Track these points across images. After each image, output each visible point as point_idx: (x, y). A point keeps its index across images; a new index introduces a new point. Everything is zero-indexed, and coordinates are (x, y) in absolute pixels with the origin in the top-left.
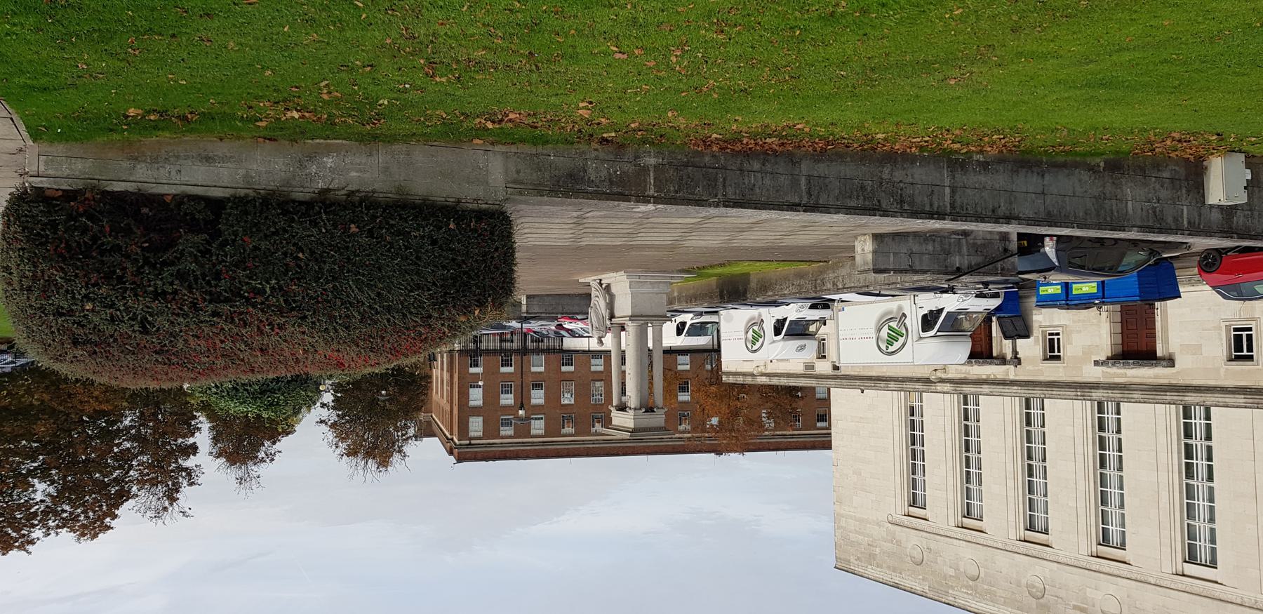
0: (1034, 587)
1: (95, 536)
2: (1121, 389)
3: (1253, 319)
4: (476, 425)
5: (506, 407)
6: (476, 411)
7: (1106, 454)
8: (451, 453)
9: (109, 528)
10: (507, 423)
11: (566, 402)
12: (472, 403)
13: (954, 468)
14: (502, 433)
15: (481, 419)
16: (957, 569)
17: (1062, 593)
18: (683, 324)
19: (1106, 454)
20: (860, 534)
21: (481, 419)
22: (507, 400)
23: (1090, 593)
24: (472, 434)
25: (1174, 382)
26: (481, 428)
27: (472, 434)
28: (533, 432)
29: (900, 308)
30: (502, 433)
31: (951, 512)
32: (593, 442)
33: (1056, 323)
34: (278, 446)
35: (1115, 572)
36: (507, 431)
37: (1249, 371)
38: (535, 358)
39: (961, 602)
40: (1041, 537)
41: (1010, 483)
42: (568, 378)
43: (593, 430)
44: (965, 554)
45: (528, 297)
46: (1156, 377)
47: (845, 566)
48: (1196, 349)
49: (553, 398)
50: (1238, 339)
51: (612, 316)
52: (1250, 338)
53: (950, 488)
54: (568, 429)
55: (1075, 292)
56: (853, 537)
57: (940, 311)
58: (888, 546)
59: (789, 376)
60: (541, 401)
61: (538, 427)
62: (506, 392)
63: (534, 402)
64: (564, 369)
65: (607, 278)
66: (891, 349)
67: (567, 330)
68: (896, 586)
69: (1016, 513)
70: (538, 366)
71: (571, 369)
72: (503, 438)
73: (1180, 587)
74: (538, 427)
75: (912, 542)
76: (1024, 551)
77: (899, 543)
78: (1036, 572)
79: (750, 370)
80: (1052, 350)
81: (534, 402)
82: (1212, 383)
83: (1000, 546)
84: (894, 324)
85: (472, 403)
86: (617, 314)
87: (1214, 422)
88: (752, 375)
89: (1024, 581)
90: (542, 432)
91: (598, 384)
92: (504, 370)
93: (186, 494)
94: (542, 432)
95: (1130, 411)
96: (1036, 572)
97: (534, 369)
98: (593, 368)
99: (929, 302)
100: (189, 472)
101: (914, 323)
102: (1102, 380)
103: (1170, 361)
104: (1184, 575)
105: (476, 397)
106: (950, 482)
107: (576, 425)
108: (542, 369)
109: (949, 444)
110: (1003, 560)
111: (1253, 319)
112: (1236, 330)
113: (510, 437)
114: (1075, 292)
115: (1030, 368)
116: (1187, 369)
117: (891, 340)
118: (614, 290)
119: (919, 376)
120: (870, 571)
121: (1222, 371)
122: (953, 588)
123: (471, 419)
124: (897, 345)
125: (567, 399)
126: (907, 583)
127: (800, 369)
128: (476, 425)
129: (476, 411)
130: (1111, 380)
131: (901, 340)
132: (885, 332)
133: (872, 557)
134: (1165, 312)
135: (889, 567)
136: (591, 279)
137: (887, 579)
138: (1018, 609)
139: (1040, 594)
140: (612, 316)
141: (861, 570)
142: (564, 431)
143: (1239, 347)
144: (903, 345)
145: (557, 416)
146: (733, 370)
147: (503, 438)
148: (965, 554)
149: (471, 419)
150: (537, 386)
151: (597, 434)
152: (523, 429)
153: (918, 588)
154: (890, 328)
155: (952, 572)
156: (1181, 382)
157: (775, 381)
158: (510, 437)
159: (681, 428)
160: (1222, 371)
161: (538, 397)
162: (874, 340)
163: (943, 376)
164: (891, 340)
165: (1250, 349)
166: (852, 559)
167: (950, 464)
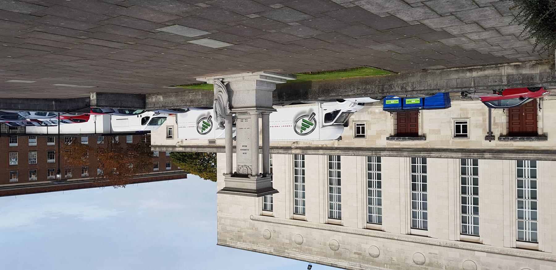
0: (333, 245)
2: (397, 151)
3: (467, 118)
7: (374, 180)
11: (13, 164)
13: (290, 191)
16: (290, 240)
17: (349, 247)
18: (148, 118)
19: (374, 180)
20: (233, 226)
23: (363, 246)
25: (425, 147)
29: (209, 113)
31: (288, 212)
32: (30, 185)
33: (362, 119)
35: (377, 235)
37: (464, 142)
39: (292, 256)
40: (378, 226)
41: (321, 196)
42: (14, 150)
43: (30, 179)
44: (296, 232)
45: (98, 94)
47: (223, 243)
48: (438, 132)
50: (458, 128)
51: (231, 107)
52: (363, 128)
53: (287, 201)
55: (407, 103)
56: (228, 228)
57: (337, 112)
58: (250, 231)
59: (198, 147)
64: (11, 145)
65: (229, 78)
66: (304, 132)
68: (255, 251)
69: (324, 210)
71: (16, 144)
73: (410, 240)
75: (264, 228)
76: (329, 228)
77: (257, 229)
78: (335, 238)
79: (174, 145)
80: (358, 132)
83: (315, 227)
84: (306, 119)
86: (234, 104)
87: (342, 162)
88: (175, 147)
89: (328, 243)
91: (33, 153)
95: (385, 161)
96: (335, 238)
98: (30, 144)
99: (331, 107)
101: (320, 117)
102: (387, 147)
103: (424, 137)
104: (411, 234)
106: (287, 197)
107: (19, 177)
109: (287, 179)
110: (316, 234)
111: (467, 118)
112: (457, 123)
114: (407, 103)
115: (347, 141)
117: (304, 127)
118: (233, 87)
119: (282, 146)
120: (239, 244)
121: (451, 142)
122: (287, 249)
124: (308, 130)
126: (262, 248)
127: (206, 143)
130: (392, 147)
131: (311, 127)
132: (300, 123)
133: (239, 238)
134: (422, 114)
135: (250, 242)
136: (210, 80)
137: (249, 247)
138: (324, 256)
139: (336, 248)
140: (231, 107)
141: (233, 245)
142: (11, 180)
144: (313, 130)
146: (160, 144)
148: (296, 232)
151: (32, 181)
153: (268, 251)
154: (304, 121)
155: (287, 241)
156: (429, 147)
157: (188, 150)
159: (83, 175)
160: (451, 142)
162: (293, 127)
163: (298, 146)
164: (304, 127)
165: (363, 132)
166: (228, 239)
167: (287, 188)
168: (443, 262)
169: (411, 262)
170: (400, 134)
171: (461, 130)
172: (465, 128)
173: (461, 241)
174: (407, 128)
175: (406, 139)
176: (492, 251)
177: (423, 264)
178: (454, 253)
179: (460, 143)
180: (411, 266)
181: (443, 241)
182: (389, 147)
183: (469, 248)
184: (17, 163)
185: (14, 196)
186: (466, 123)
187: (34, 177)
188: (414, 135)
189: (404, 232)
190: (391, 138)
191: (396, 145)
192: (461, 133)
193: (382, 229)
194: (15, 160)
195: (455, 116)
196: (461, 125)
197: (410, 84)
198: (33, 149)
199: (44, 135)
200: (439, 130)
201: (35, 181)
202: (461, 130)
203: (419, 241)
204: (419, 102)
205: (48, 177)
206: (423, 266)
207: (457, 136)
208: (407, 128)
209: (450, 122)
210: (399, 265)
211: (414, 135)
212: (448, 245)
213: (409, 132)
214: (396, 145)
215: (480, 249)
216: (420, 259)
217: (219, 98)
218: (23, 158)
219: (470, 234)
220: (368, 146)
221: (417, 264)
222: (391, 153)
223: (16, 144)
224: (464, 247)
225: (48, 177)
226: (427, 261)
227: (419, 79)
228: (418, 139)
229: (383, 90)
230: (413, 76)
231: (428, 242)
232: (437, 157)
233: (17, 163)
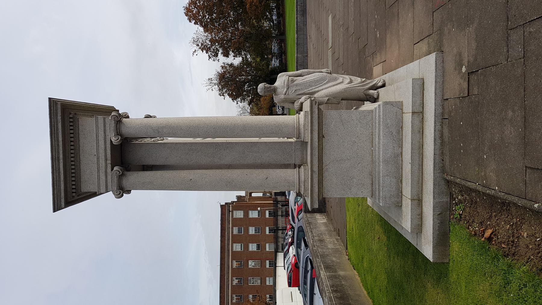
1: (187, 15)
4: (239, 214)
5: (248, 230)
6: (246, 214)
8: (226, 203)
9: (190, 21)
10: (240, 231)
11: (250, 263)
12: (250, 212)
14: (235, 228)
15: (242, 217)
21: (242, 217)
22: (252, 231)
24: (235, 212)
26: (237, 217)
27: (235, 212)
28: (235, 245)
30: (235, 228)
34: (227, 97)
36: (236, 231)
38: (273, 246)
42: (263, 264)
43: (234, 278)
49: (252, 256)
54: (235, 264)
60: (250, 249)
61: (237, 247)
62: (256, 230)
63: (250, 245)
64: (268, 262)
67: (288, 250)
70: (269, 248)
71: (268, 266)
72: (232, 228)
74: (237, 247)
81: (250, 245)
85: (250, 212)
90: (234, 250)
91: (259, 281)
92: (267, 229)
93: (204, 55)
94: (234, 250)
97: (267, 245)
98: (267, 279)
100: (216, 55)
105: (253, 214)
107: (237, 268)
108: (267, 249)
113: (232, 232)
123: (242, 212)
125: (251, 264)
128: (239, 214)
129: (246, 214)
145: (243, 257)
147: (232, 228)
149: (242, 212)
150: (258, 247)
151: (232, 280)
152: (236, 239)
158: (232, 232)
161: (253, 247)
184: (250, 267)
185: (219, 264)
187: (236, 282)
194: (253, 265)
198: (263, 281)
199: (276, 264)
201: (232, 283)
205: (234, 296)
217: (336, 79)
218: (255, 273)
223: (268, 266)
225: (234, 296)
233: (250, 267)
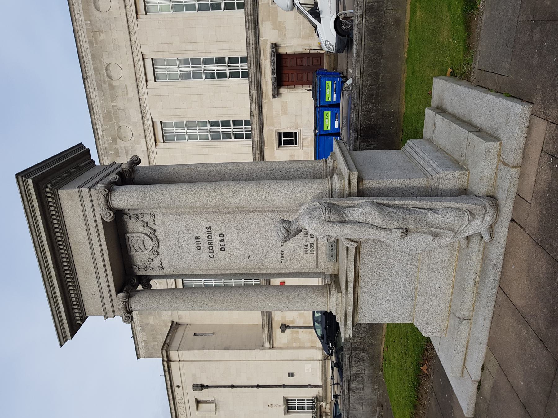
2: (256, 58)
25: (264, 96)
35: (128, 8)
37: (273, 143)
46: (266, 83)
48: (284, 112)
50: (289, 135)
55: (325, 113)
73: (136, 59)
82: (265, 121)
102: (261, 39)
103: (276, 94)
112: (296, 133)
114: (325, 113)
116: (272, 106)
121: (272, 128)
130: (262, 48)
143: (287, 135)
156: (264, 101)
160: (272, 128)
168: (120, 103)
169: (106, 60)
170: (281, 61)
171: (287, 139)
172: (290, 143)
173: (153, 123)
174: (290, 69)
175: (273, 73)
176: (151, 157)
177: (109, 77)
178: (135, 116)
179: (271, 139)
180: (101, 61)
181: (147, 102)
182: (261, 42)
183: (147, 133)
186: (296, 144)
188: (280, 82)
189: (145, 50)
190: (275, 46)
191: (265, 53)
192: (283, 139)
193: (139, 16)
195: (304, 132)
196: (294, 139)
197: (361, 386)
200: (286, 114)
202: (287, 139)
203: (138, 71)
204: (325, 129)
206: (106, 77)
207: (279, 134)
208: (290, 69)
209: (297, 127)
210: (96, 43)
211: (280, 82)
212: (143, 109)
213: (285, 72)
214: (265, 53)
215: (149, 143)
216: (115, 73)
219: (164, 131)
220: (260, 8)
221: (107, 70)
222: (252, 46)
224: (146, 127)
226: (115, 83)
227: (367, 397)
228: (273, 91)
229: (355, 349)
230: (374, 390)
231: (140, 84)
232: (251, 111)
